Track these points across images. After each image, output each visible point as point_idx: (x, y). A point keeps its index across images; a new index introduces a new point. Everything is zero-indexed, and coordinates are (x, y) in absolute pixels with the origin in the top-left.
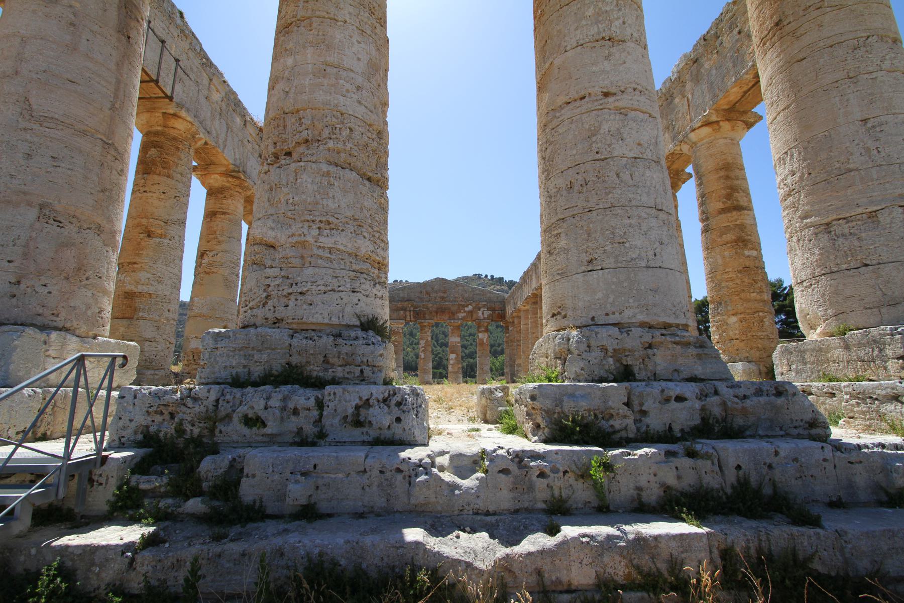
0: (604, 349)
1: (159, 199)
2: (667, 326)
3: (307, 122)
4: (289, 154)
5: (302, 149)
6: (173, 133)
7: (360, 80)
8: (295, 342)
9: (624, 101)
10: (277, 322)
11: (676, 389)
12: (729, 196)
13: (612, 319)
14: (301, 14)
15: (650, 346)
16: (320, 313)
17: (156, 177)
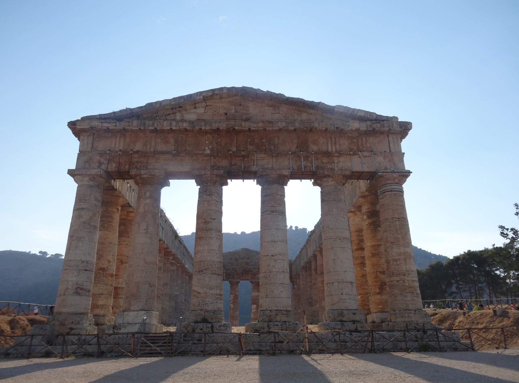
0: (267, 315)
1: (125, 247)
2: (281, 310)
3: (206, 264)
4: (202, 271)
5: (205, 271)
6: (129, 218)
7: (217, 252)
8: (206, 314)
9: (276, 258)
10: (202, 309)
11: (276, 323)
12: (359, 244)
13: (270, 309)
14: (204, 236)
15: (277, 315)
16: (210, 308)
17: (124, 238)
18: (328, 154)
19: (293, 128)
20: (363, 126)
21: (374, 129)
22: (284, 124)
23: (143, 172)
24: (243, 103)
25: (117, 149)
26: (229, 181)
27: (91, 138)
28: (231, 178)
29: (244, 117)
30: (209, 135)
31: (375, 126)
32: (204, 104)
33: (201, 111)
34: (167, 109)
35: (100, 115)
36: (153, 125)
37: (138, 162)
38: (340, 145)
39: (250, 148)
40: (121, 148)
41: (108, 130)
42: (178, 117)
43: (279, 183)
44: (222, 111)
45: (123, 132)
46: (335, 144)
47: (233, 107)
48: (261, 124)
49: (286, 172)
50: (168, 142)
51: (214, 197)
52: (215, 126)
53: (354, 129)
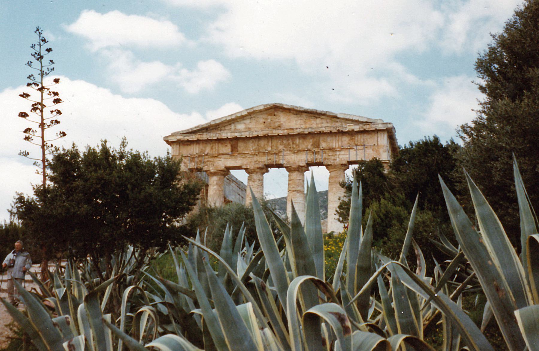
18: (331, 149)
19: (307, 133)
20: (357, 128)
21: (365, 130)
22: (301, 130)
23: (211, 169)
24: (276, 113)
25: (195, 153)
26: (269, 169)
27: (178, 146)
28: (271, 168)
29: (277, 124)
30: (253, 140)
31: (365, 127)
32: (250, 117)
33: (248, 121)
34: (225, 123)
35: (182, 131)
36: (215, 136)
37: (208, 161)
38: (342, 142)
39: (281, 147)
40: (197, 152)
41: (188, 141)
42: (233, 127)
43: (298, 171)
44: (262, 121)
45: (198, 142)
46: (338, 141)
47: (270, 117)
48: (286, 131)
49: (303, 164)
50: (226, 146)
51: (256, 183)
52: (255, 134)
53: (350, 130)
